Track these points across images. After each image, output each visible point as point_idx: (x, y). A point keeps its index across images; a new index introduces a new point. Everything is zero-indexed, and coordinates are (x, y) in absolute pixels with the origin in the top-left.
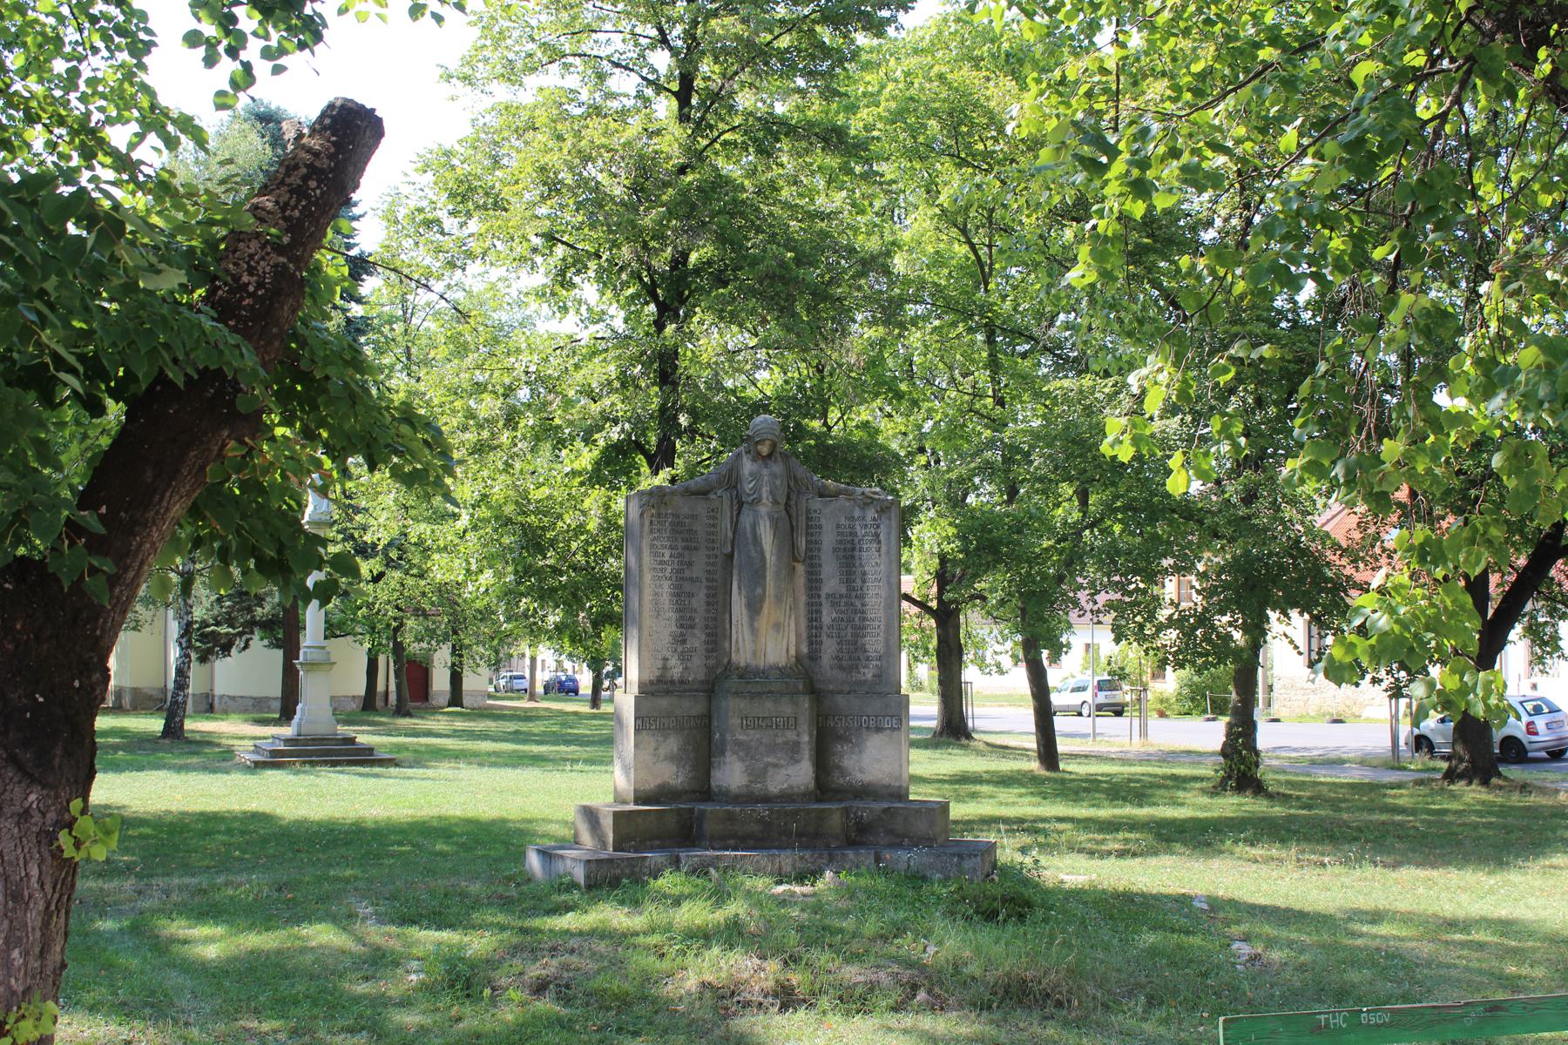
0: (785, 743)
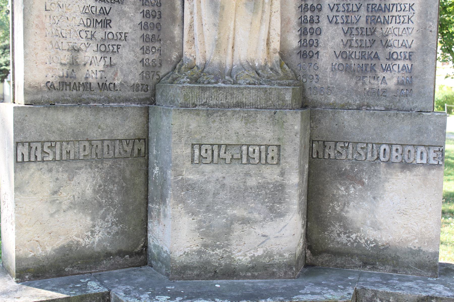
0: (261, 187)
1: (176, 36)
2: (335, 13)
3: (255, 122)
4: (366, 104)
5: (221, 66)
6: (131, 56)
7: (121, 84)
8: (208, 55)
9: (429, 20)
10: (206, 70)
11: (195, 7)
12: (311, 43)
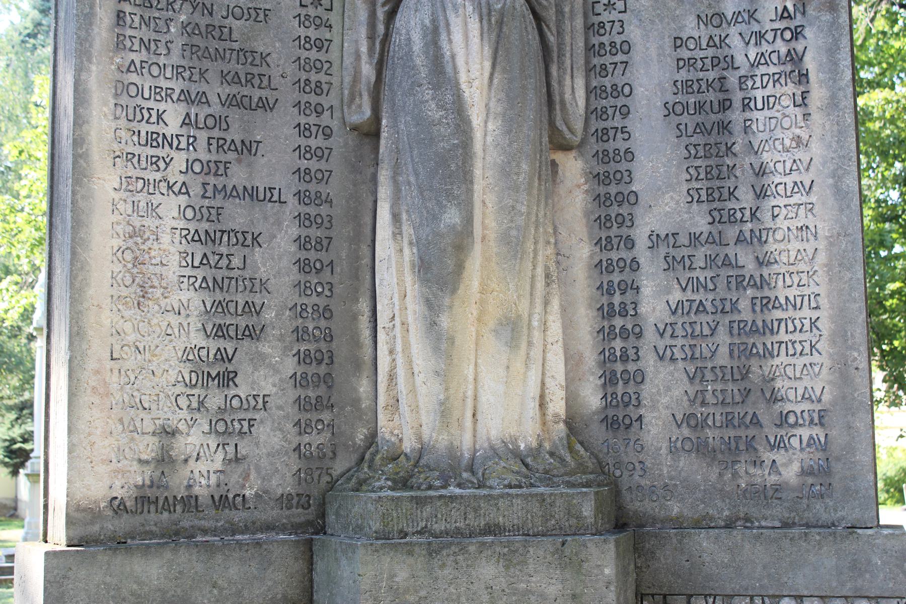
1: (364, 396)
2: (669, 341)
3: (524, 563)
4: (742, 515)
5: (452, 452)
6: (276, 440)
7: (257, 495)
8: (426, 432)
9: (851, 348)
10: (423, 462)
11: (399, 341)
12: (626, 399)
